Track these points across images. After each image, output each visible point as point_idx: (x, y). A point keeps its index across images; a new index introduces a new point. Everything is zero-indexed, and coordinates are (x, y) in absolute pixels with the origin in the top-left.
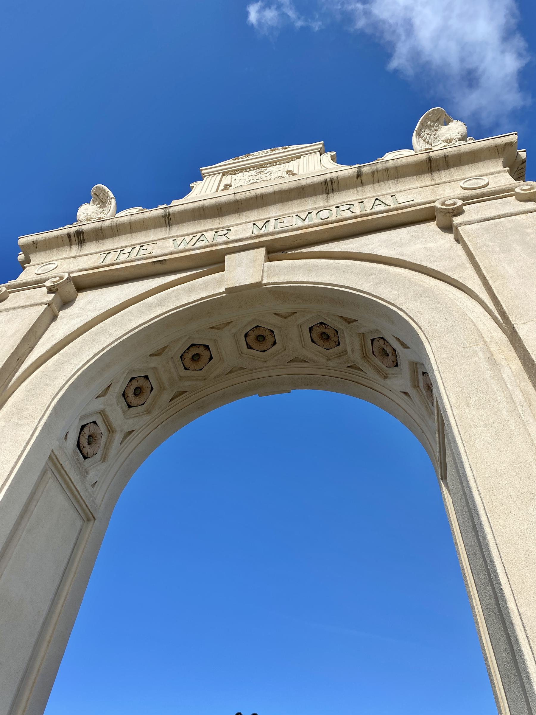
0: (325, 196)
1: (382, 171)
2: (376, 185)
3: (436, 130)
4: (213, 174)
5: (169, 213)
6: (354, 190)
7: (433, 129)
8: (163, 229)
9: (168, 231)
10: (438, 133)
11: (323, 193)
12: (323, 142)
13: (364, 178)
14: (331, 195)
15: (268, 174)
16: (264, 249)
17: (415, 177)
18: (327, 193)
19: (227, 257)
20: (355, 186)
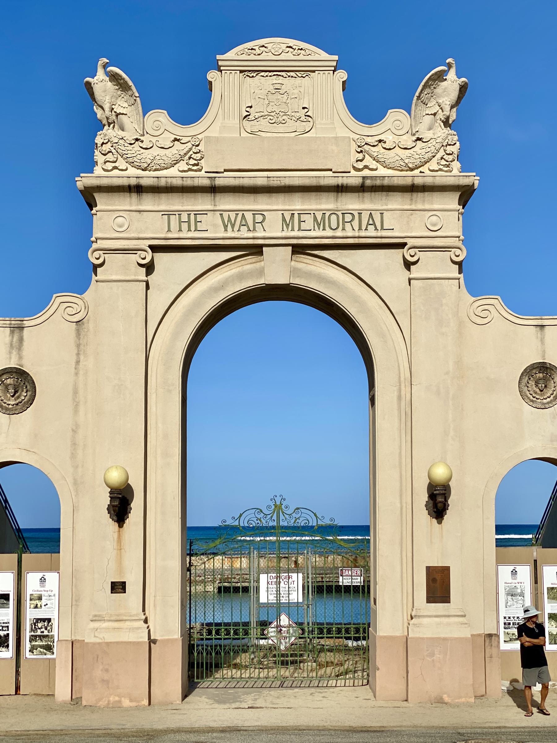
0: (335, 194)
1: (379, 186)
2: (373, 193)
3: (434, 88)
4: (231, 69)
5: (215, 185)
6: (357, 194)
7: (432, 87)
8: (209, 195)
9: (213, 197)
10: (435, 91)
11: (334, 192)
12: (336, 58)
13: (365, 188)
14: (340, 194)
15: (285, 96)
16: (291, 248)
17: (400, 193)
18: (338, 192)
19: (264, 249)
20: (358, 191)
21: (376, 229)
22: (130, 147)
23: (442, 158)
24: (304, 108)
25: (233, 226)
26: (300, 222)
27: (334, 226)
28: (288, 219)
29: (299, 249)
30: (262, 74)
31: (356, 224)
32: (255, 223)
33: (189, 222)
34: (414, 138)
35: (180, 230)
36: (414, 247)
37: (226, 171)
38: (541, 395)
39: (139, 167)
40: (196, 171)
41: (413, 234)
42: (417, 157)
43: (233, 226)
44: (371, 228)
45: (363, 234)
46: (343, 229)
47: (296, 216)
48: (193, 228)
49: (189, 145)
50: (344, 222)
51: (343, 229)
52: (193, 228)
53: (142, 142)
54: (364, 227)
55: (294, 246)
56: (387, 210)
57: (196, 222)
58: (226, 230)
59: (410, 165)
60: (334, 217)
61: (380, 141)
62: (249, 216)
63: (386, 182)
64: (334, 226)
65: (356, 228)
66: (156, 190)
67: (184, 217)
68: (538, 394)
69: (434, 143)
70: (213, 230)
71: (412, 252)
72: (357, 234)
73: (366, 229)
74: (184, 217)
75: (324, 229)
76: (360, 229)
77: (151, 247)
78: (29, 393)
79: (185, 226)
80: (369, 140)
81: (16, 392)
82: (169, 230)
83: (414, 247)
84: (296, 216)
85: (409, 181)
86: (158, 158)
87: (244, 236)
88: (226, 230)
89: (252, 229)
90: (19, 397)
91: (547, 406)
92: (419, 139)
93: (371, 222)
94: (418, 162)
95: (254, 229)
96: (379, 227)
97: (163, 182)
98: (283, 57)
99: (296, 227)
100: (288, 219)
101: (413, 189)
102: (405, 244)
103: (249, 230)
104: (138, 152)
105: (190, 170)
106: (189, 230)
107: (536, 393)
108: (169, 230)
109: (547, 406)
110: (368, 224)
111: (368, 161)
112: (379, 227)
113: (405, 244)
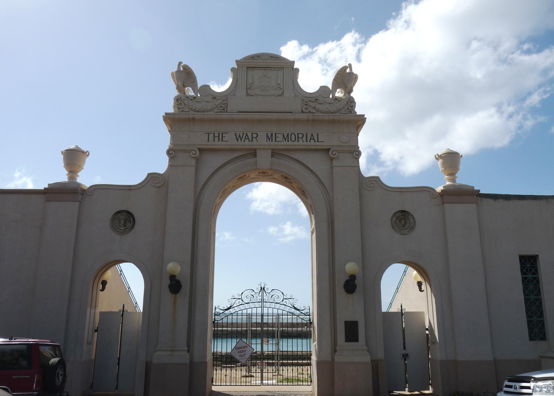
22: (191, 101)
25: (241, 139)
26: (276, 137)
27: (293, 139)
28: (269, 136)
31: (304, 138)
32: (252, 137)
33: (219, 137)
35: (214, 141)
43: (241, 139)
44: (312, 141)
45: (308, 143)
46: (298, 141)
47: (274, 135)
48: (221, 139)
49: (221, 101)
51: (298, 141)
52: (221, 139)
54: (308, 141)
55: (272, 150)
57: (222, 137)
58: (238, 141)
60: (293, 136)
61: (316, 100)
62: (250, 135)
64: (293, 139)
65: (305, 140)
66: (202, 121)
67: (217, 135)
70: (230, 140)
71: (334, 153)
72: (305, 143)
74: (217, 135)
75: (288, 141)
76: (307, 141)
77: (199, 149)
79: (216, 139)
82: (208, 141)
84: (274, 135)
88: (238, 141)
89: (251, 140)
95: (252, 141)
98: (268, 61)
99: (274, 140)
100: (269, 136)
101: (333, 122)
106: (219, 141)
108: (208, 141)
110: (311, 139)
113: (330, 149)
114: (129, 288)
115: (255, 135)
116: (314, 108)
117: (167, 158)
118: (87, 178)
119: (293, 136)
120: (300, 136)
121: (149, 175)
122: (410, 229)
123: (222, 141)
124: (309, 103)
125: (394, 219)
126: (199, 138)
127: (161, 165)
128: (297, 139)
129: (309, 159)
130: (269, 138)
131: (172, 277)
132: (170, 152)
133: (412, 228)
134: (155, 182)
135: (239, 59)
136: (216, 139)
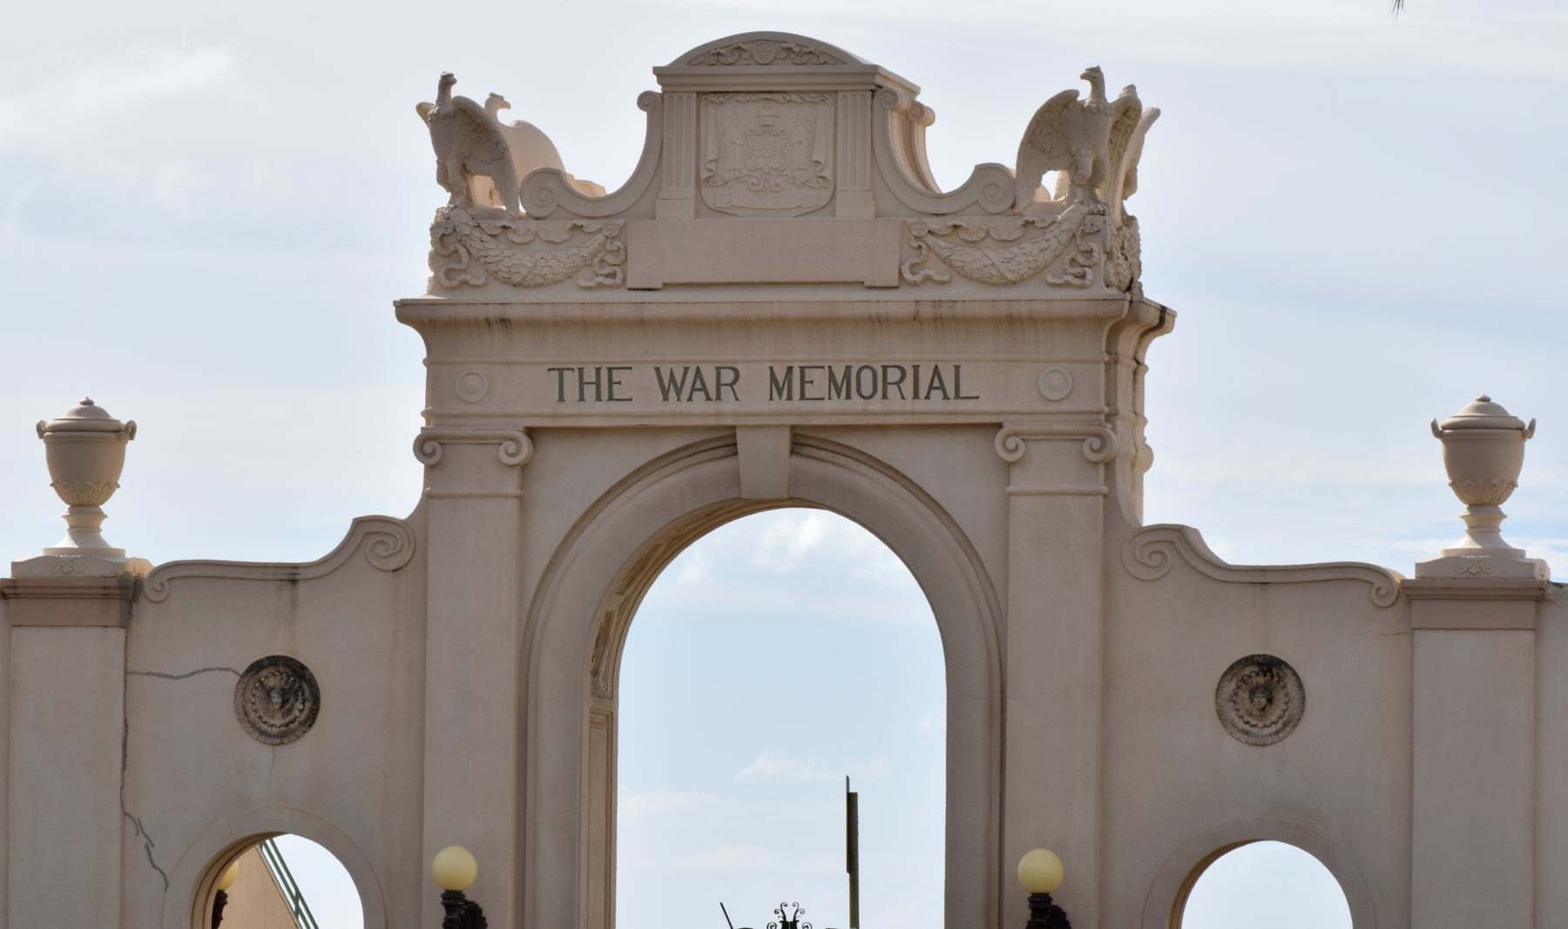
21: (946, 397)
23: (1073, 260)
24: (817, 162)
25: (679, 392)
26: (803, 382)
27: (867, 389)
29: (801, 440)
30: (740, 97)
31: (908, 386)
32: (719, 385)
33: (598, 383)
34: (1020, 222)
35: (582, 398)
36: (1016, 434)
37: (666, 286)
38: (1261, 718)
39: (507, 281)
40: (610, 287)
41: (1015, 408)
42: (1023, 259)
43: (679, 392)
46: (885, 396)
48: (605, 395)
49: (600, 238)
50: (885, 383)
51: (885, 396)
52: (605, 395)
53: (515, 231)
54: (923, 393)
55: (793, 427)
56: (968, 361)
58: (666, 398)
59: (1010, 276)
60: (867, 376)
61: (956, 227)
63: (959, 310)
64: (867, 389)
67: (590, 376)
68: (1255, 717)
69: (1056, 232)
70: (641, 398)
71: (1011, 443)
72: (910, 404)
73: (928, 397)
74: (590, 376)
76: (916, 396)
78: (308, 705)
79: (590, 391)
80: (933, 224)
81: (285, 702)
82: (561, 399)
83: (1016, 434)
85: (1002, 310)
86: (542, 263)
87: (698, 410)
88: (666, 398)
89: (713, 394)
90: (290, 711)
91: (1268, 741)
92: (1027, 224)
93: (936, 383)
94: (1024, 269)
95: (719, 398)
96: (951, 394)
97: (547, 313)
102: (999, 426)
103: (708, 398)
104: (507, 253)
105: (600, 286)
106: (598, 398)
107: (1250, 714)
108: (561, 399)
109: (1268, 741)
110: (931, 387)
111: (934, 270)
112: (951, 394)
113: (999, 426)
114: (298, 897)
115: (727, 376)
116: (947, 261)
117: (415, 472)
118: (144, 527)
119: (867, 376)
120: (894, 375)
121: (358, 523)
122: (1285, 725)
123: (611, 398)
124: (930, 239)
125: (1230, 687)
126: (523, 388)
127: (399, 490)
128: (882, 386)
129: (927, 462)
130: (778, 387)
131: (452, 899)
132: (428, 448)
133: (1291, 723)
134: (381, 550)
135: (665, 61)
136: (590, 391)
